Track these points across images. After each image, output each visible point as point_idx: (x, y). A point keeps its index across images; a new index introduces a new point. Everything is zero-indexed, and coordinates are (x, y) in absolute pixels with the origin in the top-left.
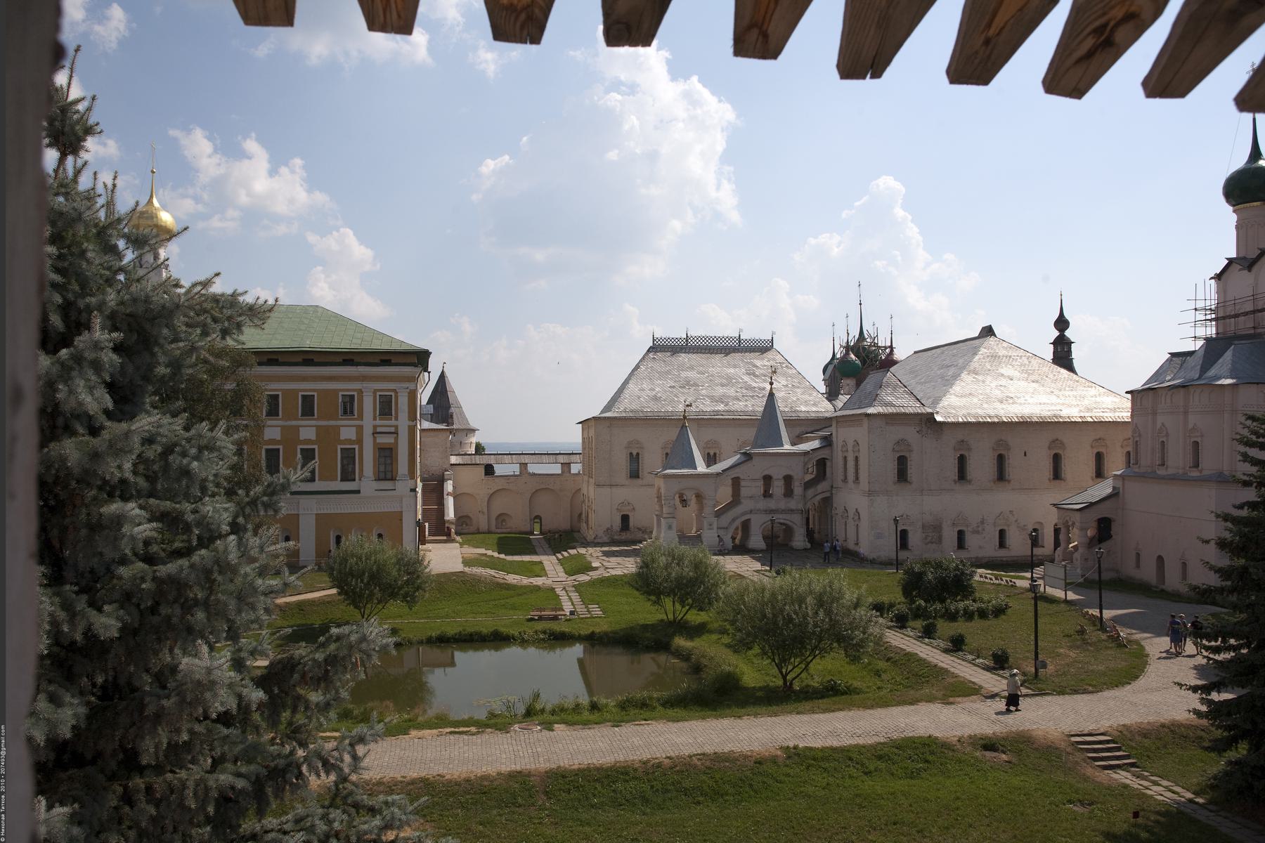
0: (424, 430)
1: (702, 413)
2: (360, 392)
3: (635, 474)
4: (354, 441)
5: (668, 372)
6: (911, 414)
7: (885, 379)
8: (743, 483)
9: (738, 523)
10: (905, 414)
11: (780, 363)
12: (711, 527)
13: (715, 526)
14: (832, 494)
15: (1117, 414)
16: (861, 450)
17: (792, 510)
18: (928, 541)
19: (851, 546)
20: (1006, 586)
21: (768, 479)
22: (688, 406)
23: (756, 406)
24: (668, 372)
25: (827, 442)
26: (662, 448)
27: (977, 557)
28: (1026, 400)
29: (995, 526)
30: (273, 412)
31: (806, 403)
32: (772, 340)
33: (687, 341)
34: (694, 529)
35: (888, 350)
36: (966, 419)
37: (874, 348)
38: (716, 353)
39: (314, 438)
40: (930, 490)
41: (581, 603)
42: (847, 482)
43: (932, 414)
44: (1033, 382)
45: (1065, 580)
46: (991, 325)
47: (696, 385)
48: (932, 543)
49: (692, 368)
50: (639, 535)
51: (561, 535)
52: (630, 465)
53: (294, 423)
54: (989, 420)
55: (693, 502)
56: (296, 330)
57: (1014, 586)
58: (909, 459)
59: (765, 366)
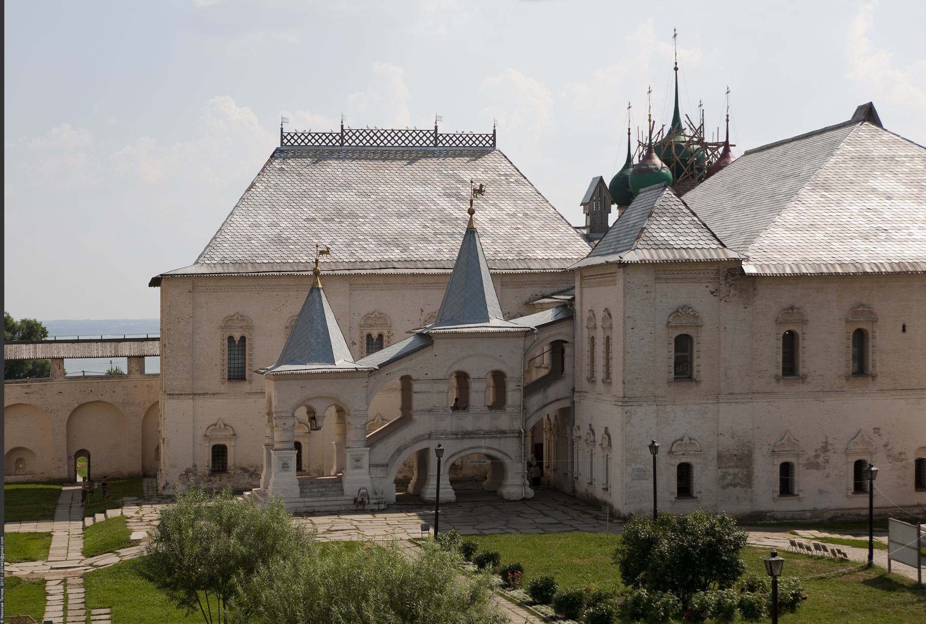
1: (359, 265)
3: (237, 374)
5: (305, 194)
6: (699, 262)
7: (659, 202)
8: (416, 387)
9: (410, 455)
10: (688, 262)
12: (359, 464)
13: (365, 462)
14: (573, 403)
16: (614, 326)
17: (503, 432)
18: (727, 481)
19: (599, 494)
20: (830, 560)
21: (462, 378)
22: (322, 253)
24: (305, 194)
25: (568, 312)
26: (222, 328)
27: (815, 510)
28: (910, 234)
29: (847, 455)
31: (546, 245)
33: (342, 137)
34: (335, 468)
35: (721, 150)
36: (798, 268)
37: (696, 147)
38: (394, 159)
40: (732, 394)
41: (83, 606)
42: (610, 383)
45: (919, 549)
46: (871, 103)
47: (353, 215)
48: (735, 486)
49: (347, 186)
50: (244, 480)
51: (103, 484)
52: (229, 359)
54: (839, 270)
55: (329, 419)
57: (844, 560)
58: (695, 340)
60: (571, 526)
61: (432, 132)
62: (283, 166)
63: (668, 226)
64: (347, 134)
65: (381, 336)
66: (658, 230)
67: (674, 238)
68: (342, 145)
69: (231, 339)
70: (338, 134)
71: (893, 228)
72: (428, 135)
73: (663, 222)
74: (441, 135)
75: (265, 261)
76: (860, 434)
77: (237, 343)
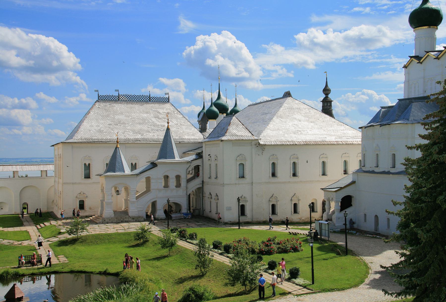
3: (87, 176)
6: (246, 140)
8: (152, 181)
15: (354, 140)
21: (166, 178)
24: (108, 116)
25: (200, 156)
32: (169, 98)
36: (276, 143)
43: (257, 140)
44: (311, 122)
47: (124, 123)
49: (122, 113)
52: (85, 171)
54: (288, 143)
60: (208, 225)
63: (235, 129)
64: (120, 96)
66: (232, 130)
67: (237, 132)
69: (85, 164)
70: (117, 96)
71: (302, 130)
72: (147, 97)
73: (234, 127)
75: (96, 138)
76: (295, 195)
77: (87, 166)
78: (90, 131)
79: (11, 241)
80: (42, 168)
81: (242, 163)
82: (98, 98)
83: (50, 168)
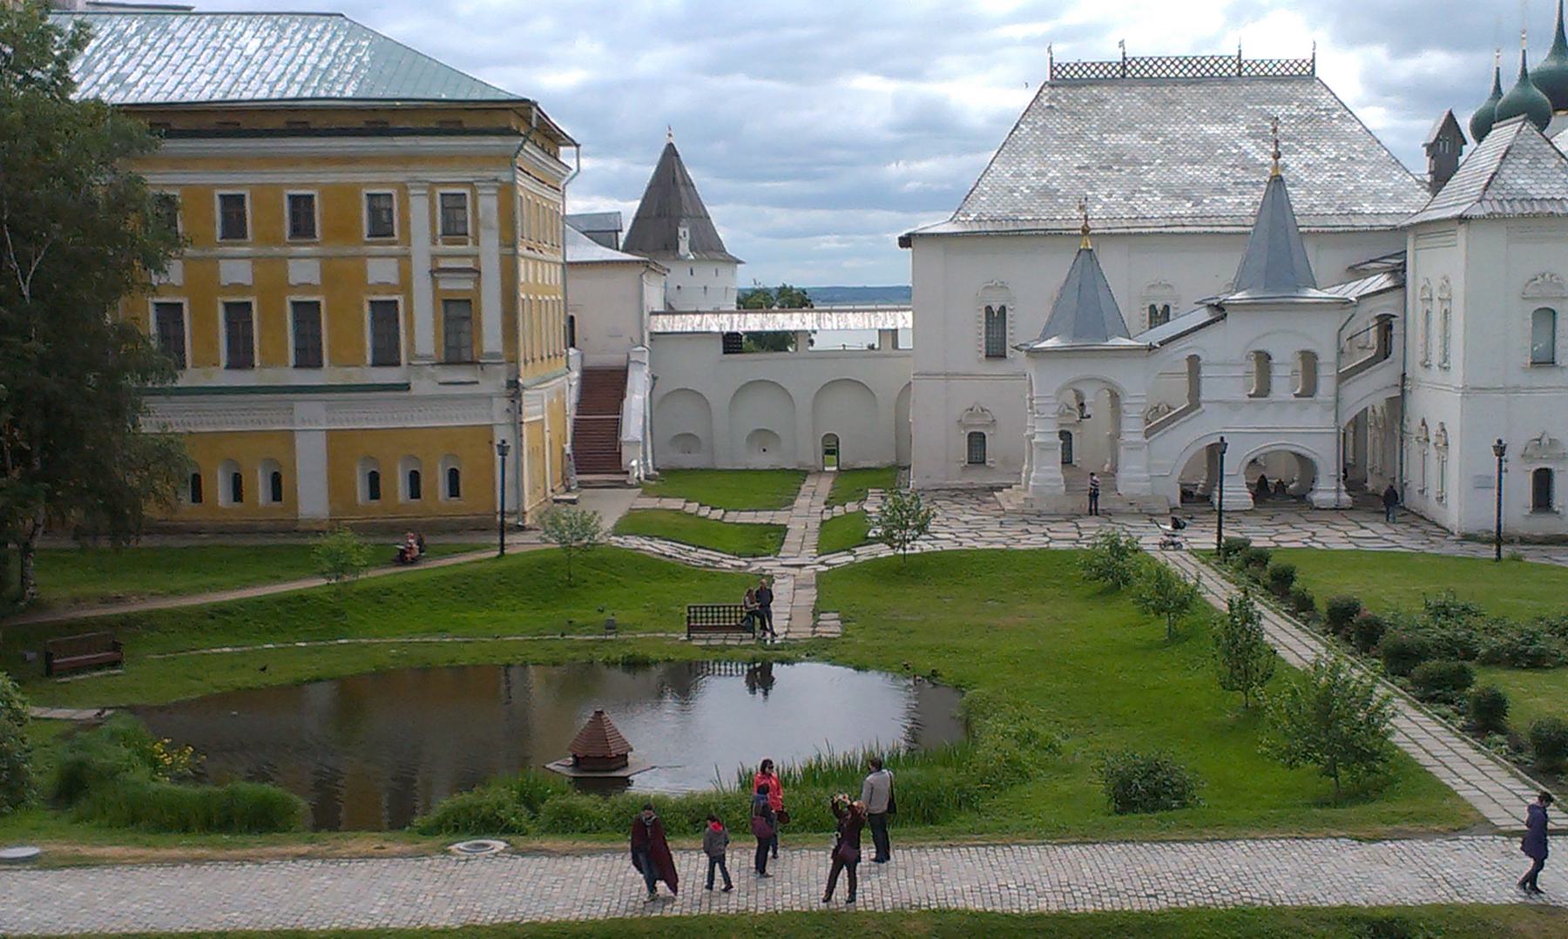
0: (571, 264)
2: (403, 188)
4: (394, 286)
5: (1079, 136)
8: (1205, 372)
11: (1325, 109)
14: (1403, 391)
21: (1263, 359)
23: (1243, 204)
24: (1079, 136)
30: (234, 228)
31: (1377, 196)
39: (316, 281)
47: (1135, 162)
49: (1129, 127)
52: (987, 333)
53: (277, 250)
56: (229, 72)
59: (1292, 117)
60: (1393, 542)
61: (1234, 59)
62: (1053, 104)
64: (1129, 63)
65: (1167, 307)
68: (1123, 76)
69: (989, 308)
70: (1118, 63)
72: (1230, 62)
74: (1246, 61)
75: (1030, 218)
77: (996, 314)
78: (1011, 191)
79: (716, 556)
80: (889, 320)
81: (1540, 309)
82: (1052, 75)
83: (903, 321)
